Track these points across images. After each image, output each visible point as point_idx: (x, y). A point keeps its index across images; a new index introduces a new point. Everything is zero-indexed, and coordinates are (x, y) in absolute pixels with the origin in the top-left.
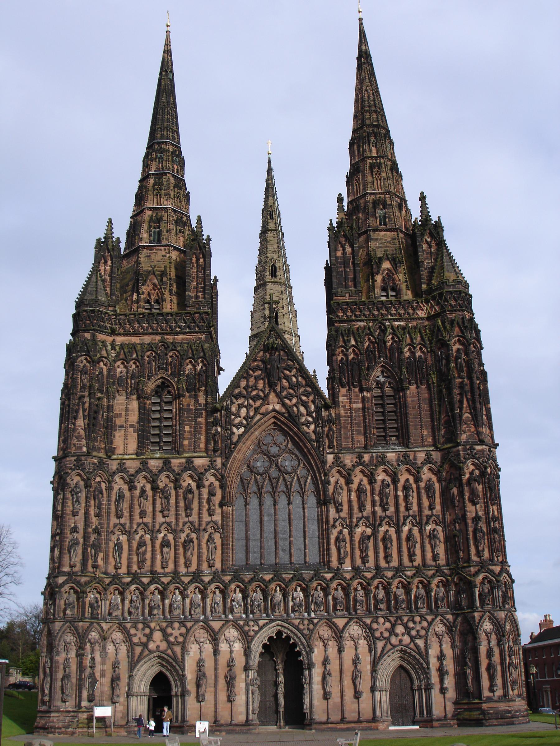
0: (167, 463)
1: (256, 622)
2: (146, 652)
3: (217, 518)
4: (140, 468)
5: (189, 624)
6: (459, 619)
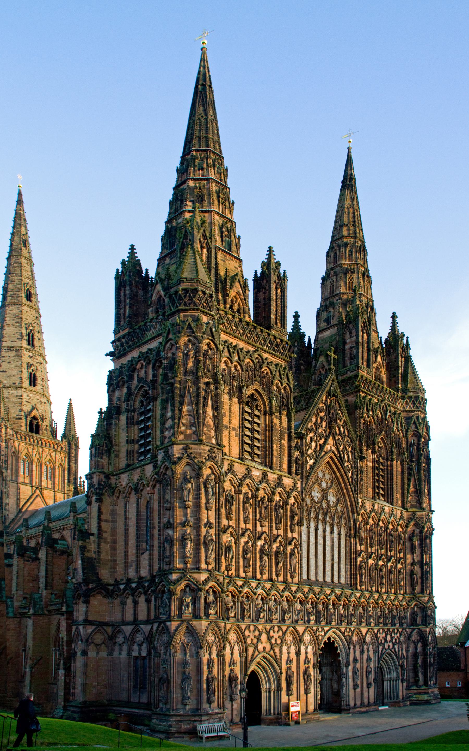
0: (265, 475)
1: (323, 629)
2: (257, 653)
3: (295, 535)
4: (246, 474)
5: (284, 628)
6: (415, 631)
